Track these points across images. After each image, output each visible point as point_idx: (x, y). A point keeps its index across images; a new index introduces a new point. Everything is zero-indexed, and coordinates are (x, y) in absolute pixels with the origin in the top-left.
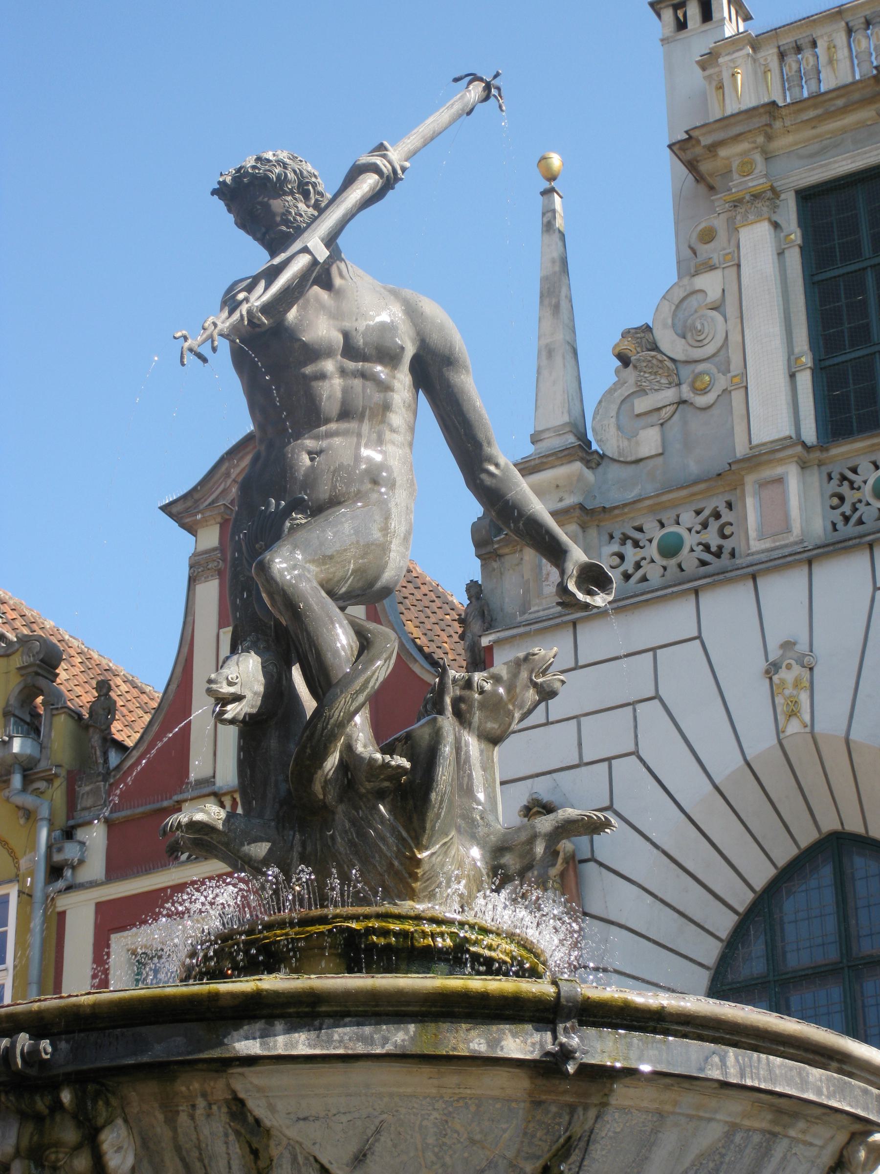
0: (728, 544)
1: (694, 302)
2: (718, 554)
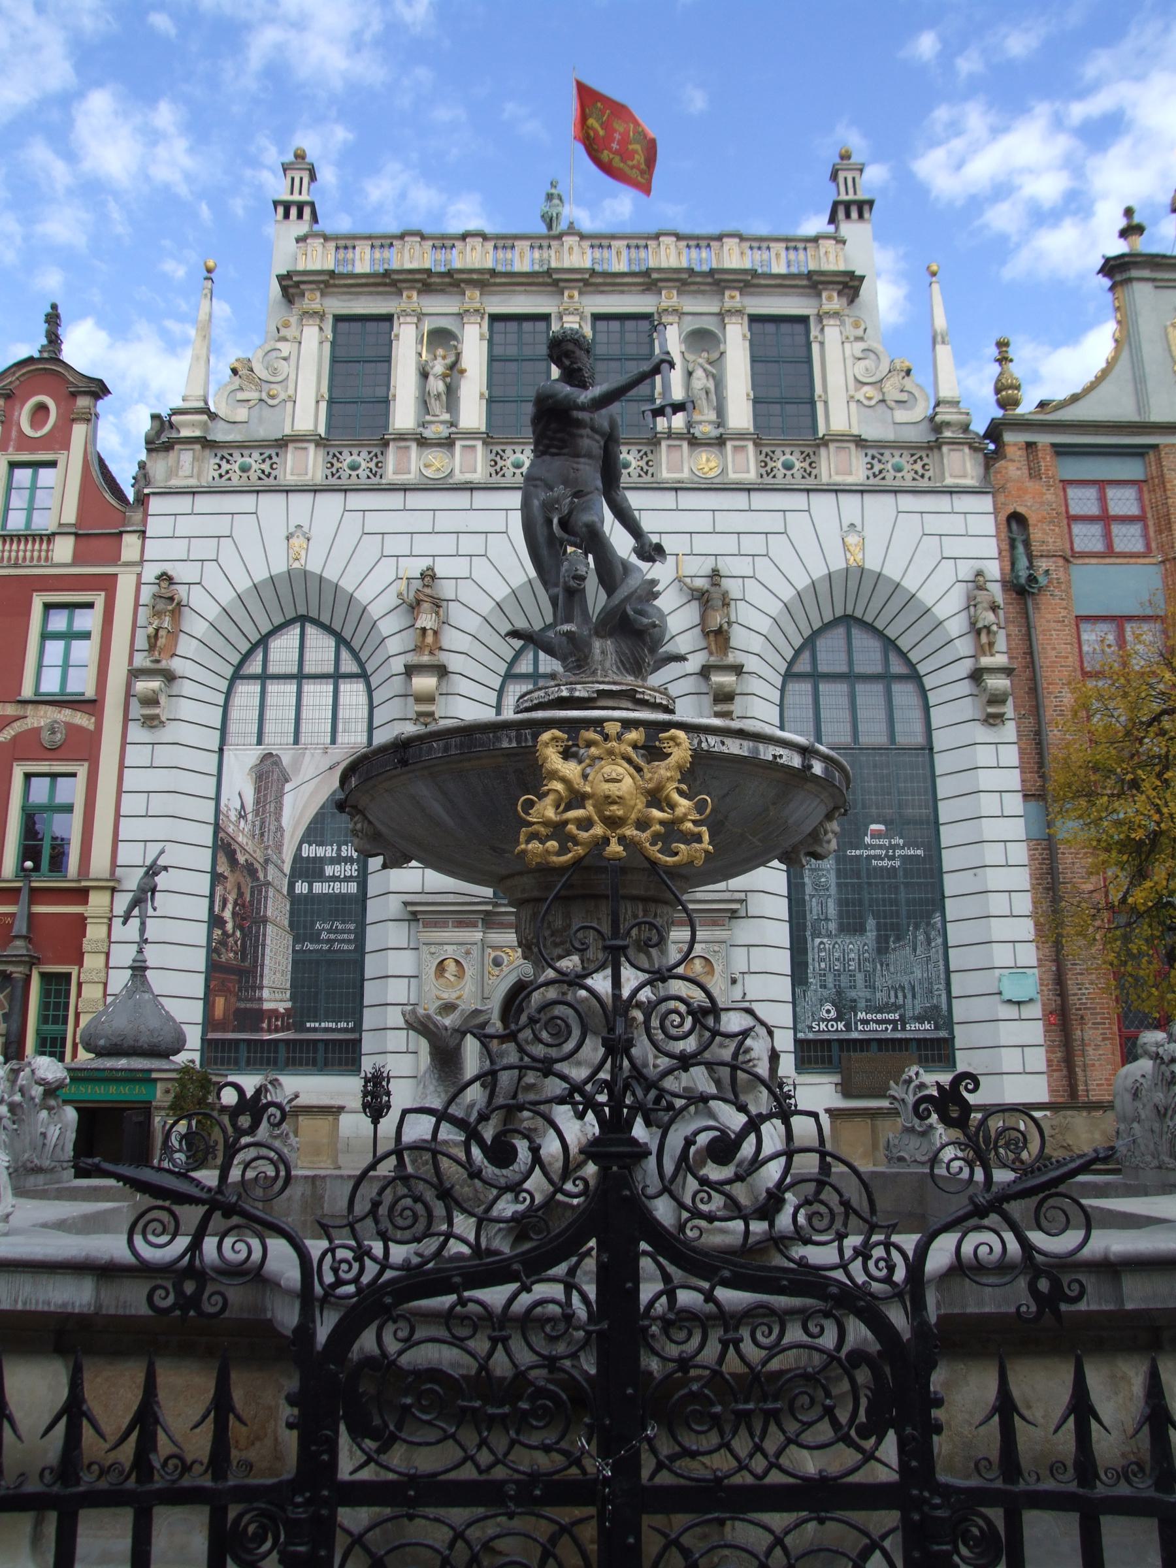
0: (274, 473)
1: (274, 354)
2: (268, 476)
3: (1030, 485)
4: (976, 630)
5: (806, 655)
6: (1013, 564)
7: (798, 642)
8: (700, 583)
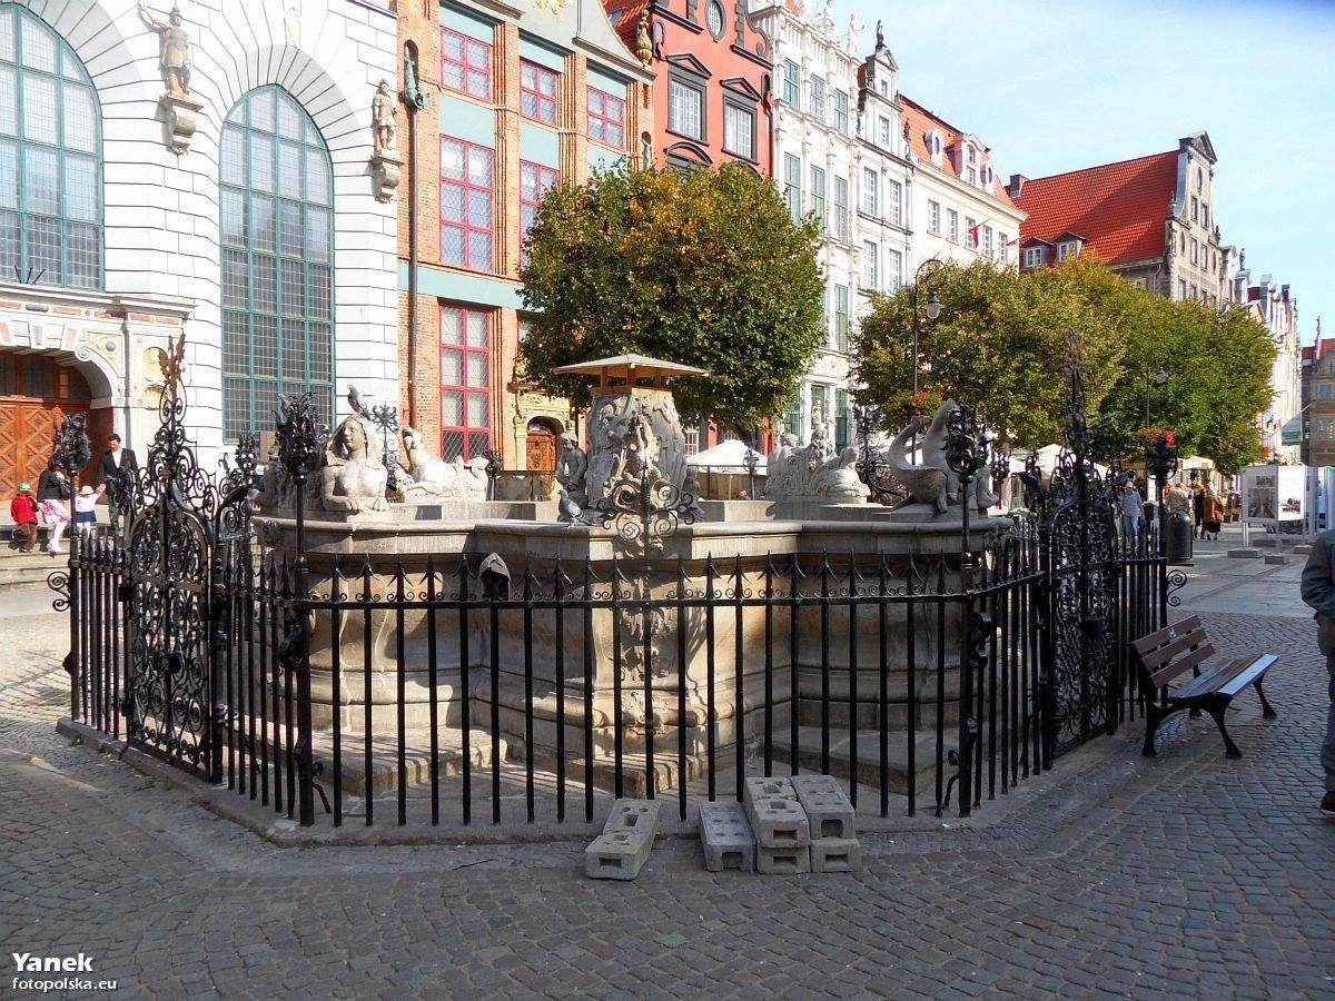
3: (423, 22)
4: (377, 127)
5: (239, 108)
6: (406, 83)
7: (237, 97)
8: (164, 20)
